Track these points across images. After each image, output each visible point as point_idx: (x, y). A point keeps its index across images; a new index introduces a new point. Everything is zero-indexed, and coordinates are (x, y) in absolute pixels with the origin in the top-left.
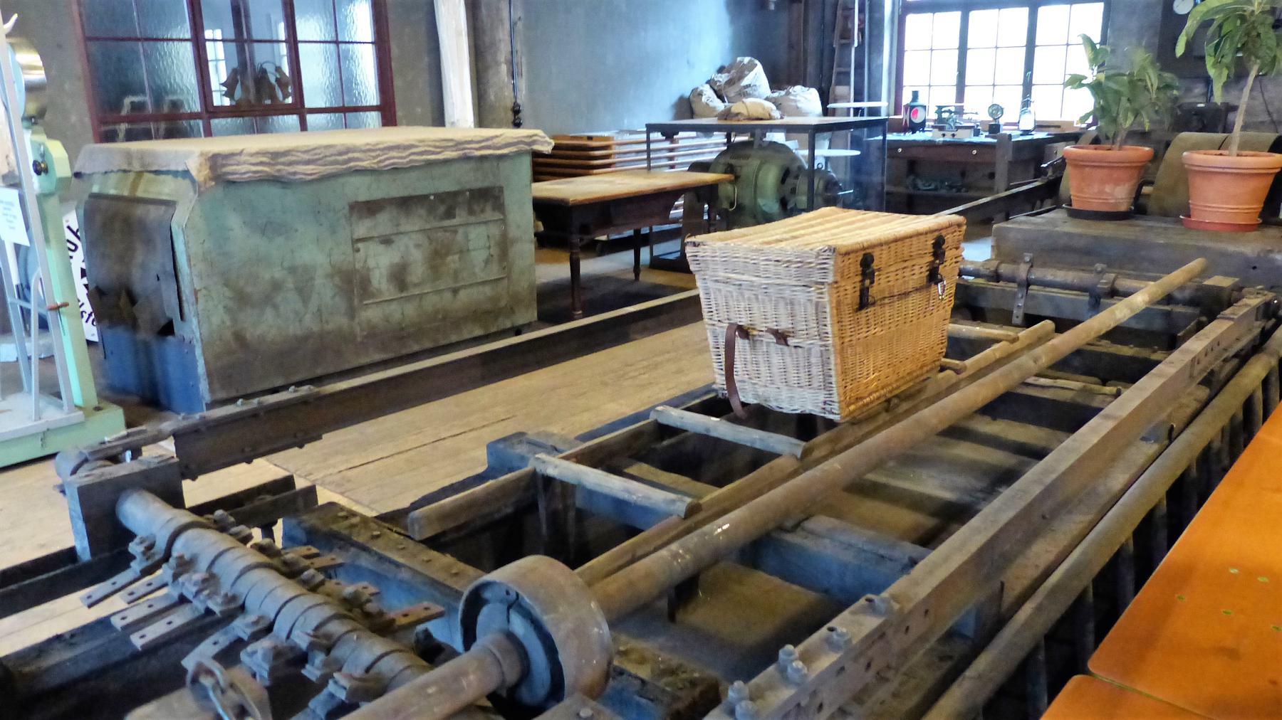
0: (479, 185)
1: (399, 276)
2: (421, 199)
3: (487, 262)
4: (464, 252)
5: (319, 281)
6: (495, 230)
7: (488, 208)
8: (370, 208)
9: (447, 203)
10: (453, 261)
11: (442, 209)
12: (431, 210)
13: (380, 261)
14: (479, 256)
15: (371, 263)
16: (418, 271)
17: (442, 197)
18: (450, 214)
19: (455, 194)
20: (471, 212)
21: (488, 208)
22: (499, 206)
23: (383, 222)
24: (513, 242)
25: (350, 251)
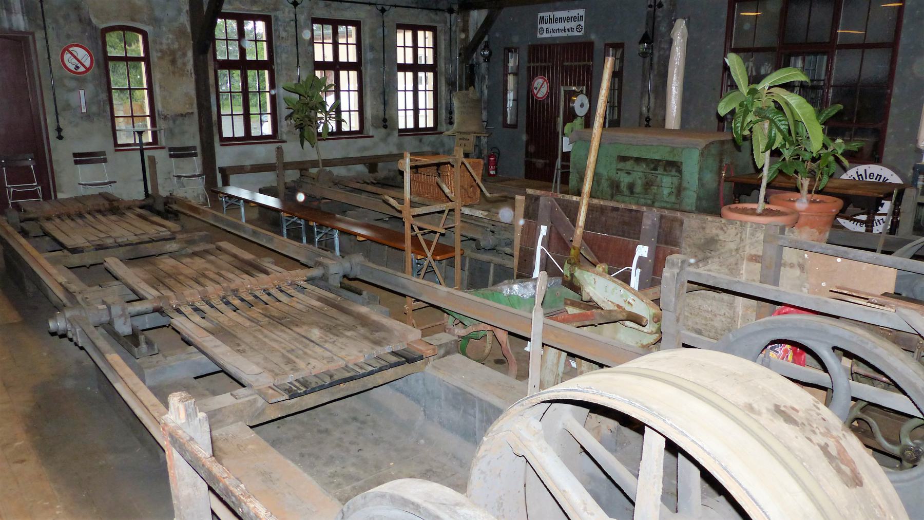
0: (670, 159)
1: (631, 187)
2: (645, 160)
3: (670, 194)
4: (659, 186)
5: (603, 181)
6: (676, 180)
7: (674, 170)
8: (623, 159)
9: (655, 164)
10: (654, 189)
11: (652, 166)
12: (647, 166)
13: (625, 180)
14: (666, 192)
15: (622, 180)
16: (638, 189)
17: (653, 161)
18: (655, 169)
19: (659, 161)
20: (665, 170)
21: (674, 170)
22: (679, 171)
23: (629, 165)
24: (685, 189)
25: (615, 172)
